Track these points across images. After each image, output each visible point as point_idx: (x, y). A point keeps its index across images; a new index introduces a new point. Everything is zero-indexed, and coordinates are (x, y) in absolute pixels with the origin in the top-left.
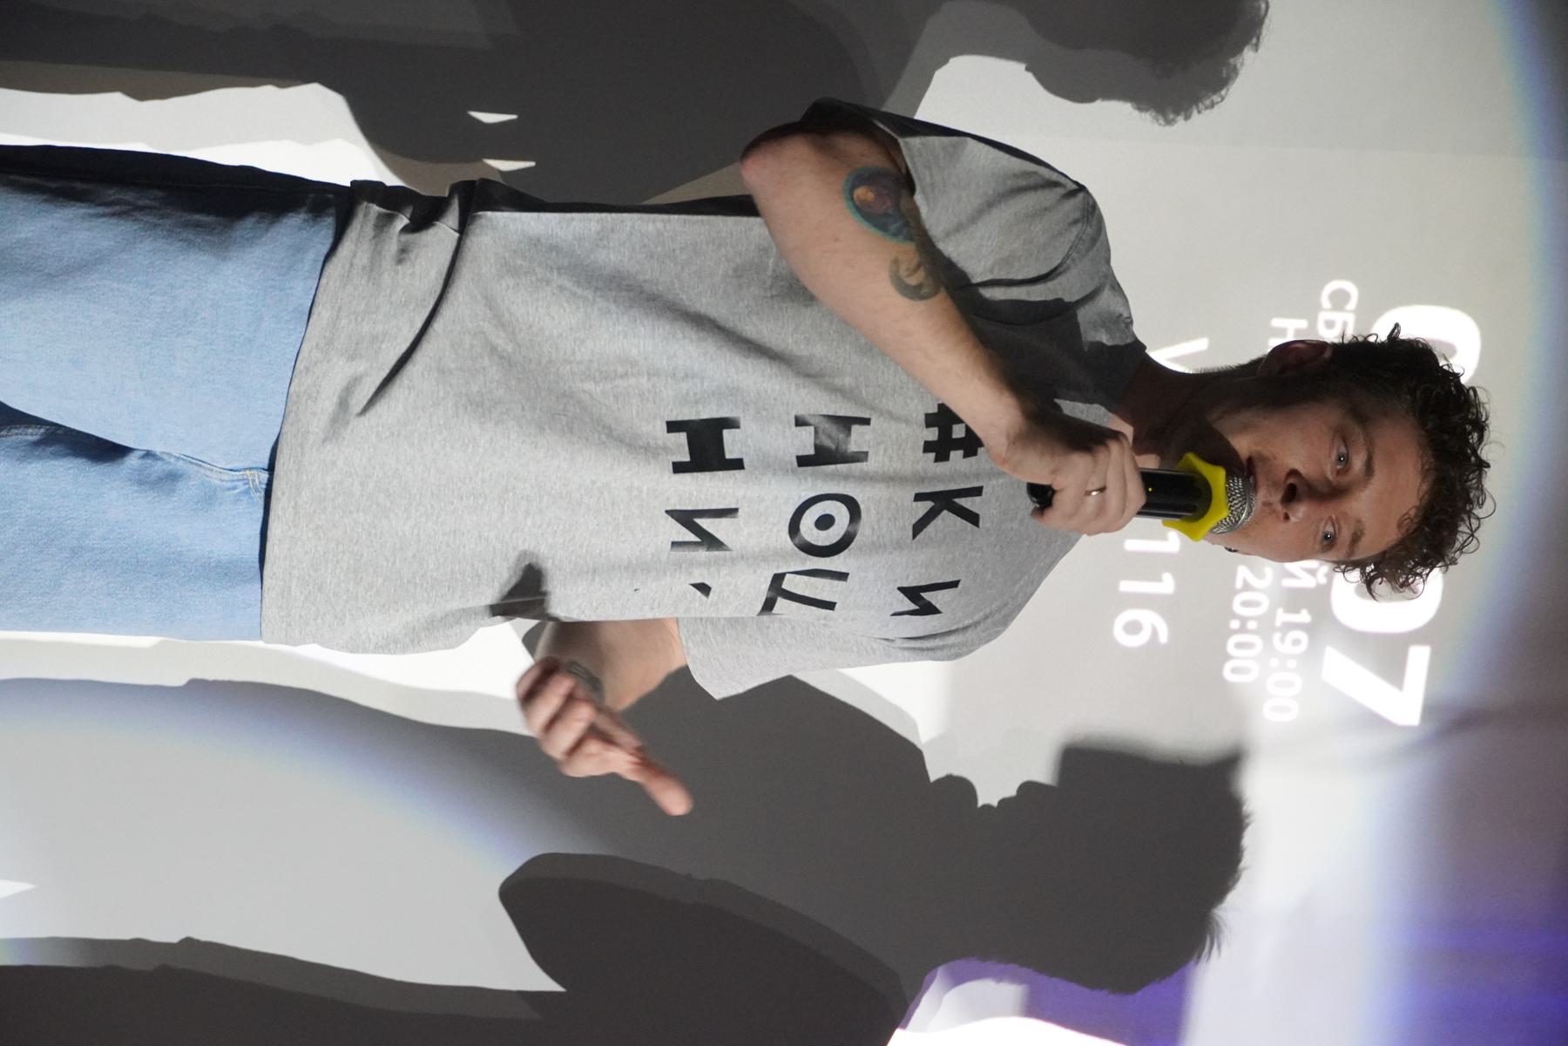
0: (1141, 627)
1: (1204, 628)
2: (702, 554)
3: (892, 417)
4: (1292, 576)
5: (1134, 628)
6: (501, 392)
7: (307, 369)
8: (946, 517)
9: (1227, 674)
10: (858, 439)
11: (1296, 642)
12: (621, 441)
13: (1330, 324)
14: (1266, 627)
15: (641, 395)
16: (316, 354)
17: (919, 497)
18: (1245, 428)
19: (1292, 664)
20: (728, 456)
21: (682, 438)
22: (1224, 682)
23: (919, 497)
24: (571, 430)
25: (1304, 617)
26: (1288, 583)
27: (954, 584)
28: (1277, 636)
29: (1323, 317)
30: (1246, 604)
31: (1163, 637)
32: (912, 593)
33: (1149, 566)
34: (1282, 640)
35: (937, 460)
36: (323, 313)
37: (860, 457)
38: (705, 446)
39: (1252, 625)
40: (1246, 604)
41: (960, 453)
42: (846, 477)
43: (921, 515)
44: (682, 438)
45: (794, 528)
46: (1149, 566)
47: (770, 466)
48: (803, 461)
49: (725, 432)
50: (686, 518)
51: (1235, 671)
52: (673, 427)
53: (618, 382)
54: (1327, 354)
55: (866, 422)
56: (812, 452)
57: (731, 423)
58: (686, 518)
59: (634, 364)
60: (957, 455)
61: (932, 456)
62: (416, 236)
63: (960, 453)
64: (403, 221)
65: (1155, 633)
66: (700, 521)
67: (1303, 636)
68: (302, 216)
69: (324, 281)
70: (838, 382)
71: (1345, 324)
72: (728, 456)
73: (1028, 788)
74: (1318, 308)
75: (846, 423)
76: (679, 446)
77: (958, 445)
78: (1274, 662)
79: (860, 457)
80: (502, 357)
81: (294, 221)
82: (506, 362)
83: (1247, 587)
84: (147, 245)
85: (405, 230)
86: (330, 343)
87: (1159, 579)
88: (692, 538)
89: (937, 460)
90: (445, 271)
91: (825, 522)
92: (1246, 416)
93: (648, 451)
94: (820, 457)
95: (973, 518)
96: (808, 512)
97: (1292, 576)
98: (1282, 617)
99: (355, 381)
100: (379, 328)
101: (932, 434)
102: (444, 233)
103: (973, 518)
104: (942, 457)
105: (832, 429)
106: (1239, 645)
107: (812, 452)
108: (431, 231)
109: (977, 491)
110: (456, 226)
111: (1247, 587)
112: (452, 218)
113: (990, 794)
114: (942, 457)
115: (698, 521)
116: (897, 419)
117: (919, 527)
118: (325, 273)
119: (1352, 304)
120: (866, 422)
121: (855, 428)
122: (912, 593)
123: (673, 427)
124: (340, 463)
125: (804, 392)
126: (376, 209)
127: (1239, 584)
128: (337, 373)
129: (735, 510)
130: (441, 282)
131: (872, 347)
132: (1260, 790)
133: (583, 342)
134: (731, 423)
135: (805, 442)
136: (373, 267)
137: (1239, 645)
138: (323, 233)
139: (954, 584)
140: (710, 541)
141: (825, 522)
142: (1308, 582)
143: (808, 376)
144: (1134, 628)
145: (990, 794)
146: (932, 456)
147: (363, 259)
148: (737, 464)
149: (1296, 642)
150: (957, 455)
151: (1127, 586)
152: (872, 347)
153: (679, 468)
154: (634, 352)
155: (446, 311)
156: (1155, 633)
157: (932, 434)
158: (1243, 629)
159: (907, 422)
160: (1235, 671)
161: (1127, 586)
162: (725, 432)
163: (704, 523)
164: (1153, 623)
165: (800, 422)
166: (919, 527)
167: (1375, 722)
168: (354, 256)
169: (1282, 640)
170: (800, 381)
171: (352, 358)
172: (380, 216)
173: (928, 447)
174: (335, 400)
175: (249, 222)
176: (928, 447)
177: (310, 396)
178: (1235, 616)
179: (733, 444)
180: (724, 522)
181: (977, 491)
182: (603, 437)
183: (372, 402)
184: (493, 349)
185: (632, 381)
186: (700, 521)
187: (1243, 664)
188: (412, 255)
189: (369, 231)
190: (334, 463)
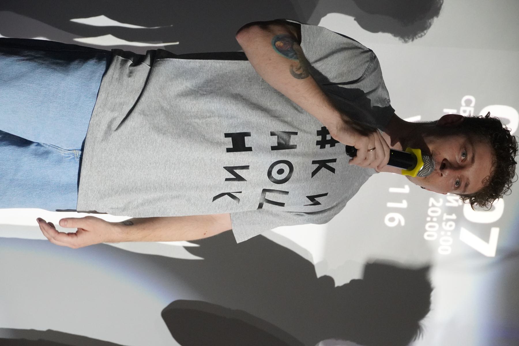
0: (395, 220)
1: (417, 219)
2: (236, 183)
3: (305, 131)
4: (449, 202)
5: (392, 220)
6: (165, 123)
7: (97, 115)
8: (323, 170)
9: (426, 237)
10: (293, 140)
11: (451, 226)
12: (208, 141)
13: (465, 111)
14: (440, 220)
15: (216, 124)
16: (100, 110)
17: (314, 162)
18: (431, 142)
19: (449, 233)
20: (246, 146)
21: (230, 139)
22: (424, 239)
23: (314, 162)
24: (190, 136)
25: (454, 217)
26: (448, 204)
27: (326, 194)
28: (444, 224)
29: (462, 109)
30: (433, 212)
31: (403, 223)
32: (311, 198)
33: (398, 198)
34: (446, 225)
35: (321, 148)
36: (102, 95)
37: (293, 147)
38: (239, 142)
39: (435, 219)
40: (433, 212)
41: (329, 145)
42: (288, 154)
43: (315, 169)
44: (230, 139)
45: (269, 174)
46: (398, 198)
47: (261, 149)
48: (273, 148)
49: (246, 137)
50: (230, 169)
51: (428, 236)
52: (227, 135)
53: (208, 119)
54: (462, 120)
55: (296, 133)
56: (277, 145)
57: (248, 134)
58: (230, 169)
59: (213, 113)
60: (328, 146)
61: (319, 146)
62: (135, 67)
63: (329, 145)
64: (130, 62)
65: (400, 222)
66: (236, 171)
67: (453, 224)
68: (95, 60)
69: (102, 83)
70: (286, 119)
71: (470, 112)
72: (246, 146)
73: (353, 282)
74: (460, 105)
75: (290, 133)
76: (229, 143)
77: (328, 142)
78: (443, 233)
79: (293, 147)
80: (165, 111)
81: (92, 62)
82: (167, 113)
83: (433, 206)
84: (39, 70)
85: (131, 65)
86: (105, 105)
87: (401, 202)
88: (233, 177)
89: (321, 148)
90: (145, 80)
91: (281, 172)
92: (431, 138)
93: (219, 144)
94: (280, 147)
95: (333, 170)
96: (274, 168)
97: (449, 202)
98: (446, 217)
99: (114, 119)
100: (122, 100)
101: (319, 138)
102: (145, 67)
103: (333, 170)
104: (323, 147)
105: (285, 136)
106: (430, 227)
107: (277, 145)
108: (141, 66)
109: (334, 160)
110: (149, 64)
111: (433, 206)
112: (148, 62)
113: (339, 282)
114: (323, 147)
115: (235, 170)
116: (307, 133)
117: (314, 173)
118: (103, 81)
119: (473, 104)
120: (296, 133)
121: (292, 136)
122: (311, 198)
123: (227, 135)
124: (107, 149)
125: (274, 123)
126: (121, 58)
127: (430, 205)
128: (108, 116)
129: (248, 166)
130: (144, 84)
131: (297, 108)
132: (437, 279)
133: (195, 105)
134: (248, 134)
135: (274, 141)
136: (120, 79)
137: (430, 227)
138: (102, 67)
139: (326, 194)
140: (239, 178)
141: (281, 172)
142: (455, 204)
143: (275, 117)
144: (392, 220)
145: (339, 282)
146: (319, 146)
147: (116, 76)
148: (250, 149)
149: (451, 226)
150: (328, 146)
151: (390, 205)
152: (297, 108)
153: (229, 150)
154: (213, 108)
155: (146, 94)
156: (400, 222)
157: (319, 138)
158: (431, 221)
159: (310, 133)
160: (428, 236)
161: (390, 205)
162: (246, 137)
163: (237, 171)
164: (399, 219)
165: (272, 134)
166: (314, 173)
167: (478, 255)
168: (113, 74)
169: (446, 225)
170: (272, 118)
171: (112, 111)
172: (122, 60)
173: (318, 143)
174: (106, 126)
175: (76, 62)
176: (318, 143)
177: (97, 124)
178: (429, 216)
179: (248, 142)
180: (244, 171)
181: (334, 160)
182: (202, 139)
183: (117, 129)
184: (162, 108)
185: (213, 119)
186: (236, 171)
187: (431, 233)
188: (134, 74)
189: (118, 65)
190: (105, 149)
